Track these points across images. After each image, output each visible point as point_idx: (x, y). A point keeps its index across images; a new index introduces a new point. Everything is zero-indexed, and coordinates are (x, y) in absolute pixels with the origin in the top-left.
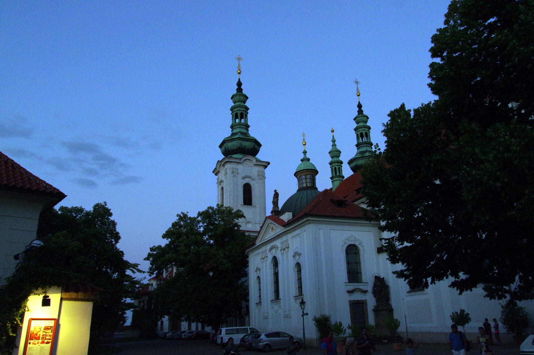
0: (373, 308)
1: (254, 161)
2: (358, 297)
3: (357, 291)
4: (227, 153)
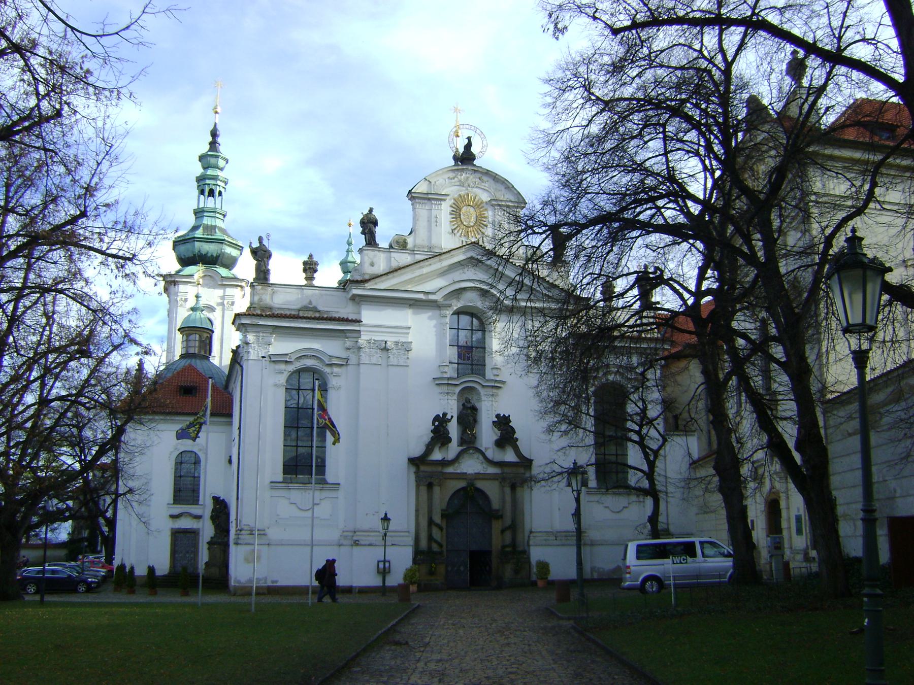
0: (209, 539)
1: (218, 278)
2: (185, 523)
3: (186, 516)
4: (185, 261)
